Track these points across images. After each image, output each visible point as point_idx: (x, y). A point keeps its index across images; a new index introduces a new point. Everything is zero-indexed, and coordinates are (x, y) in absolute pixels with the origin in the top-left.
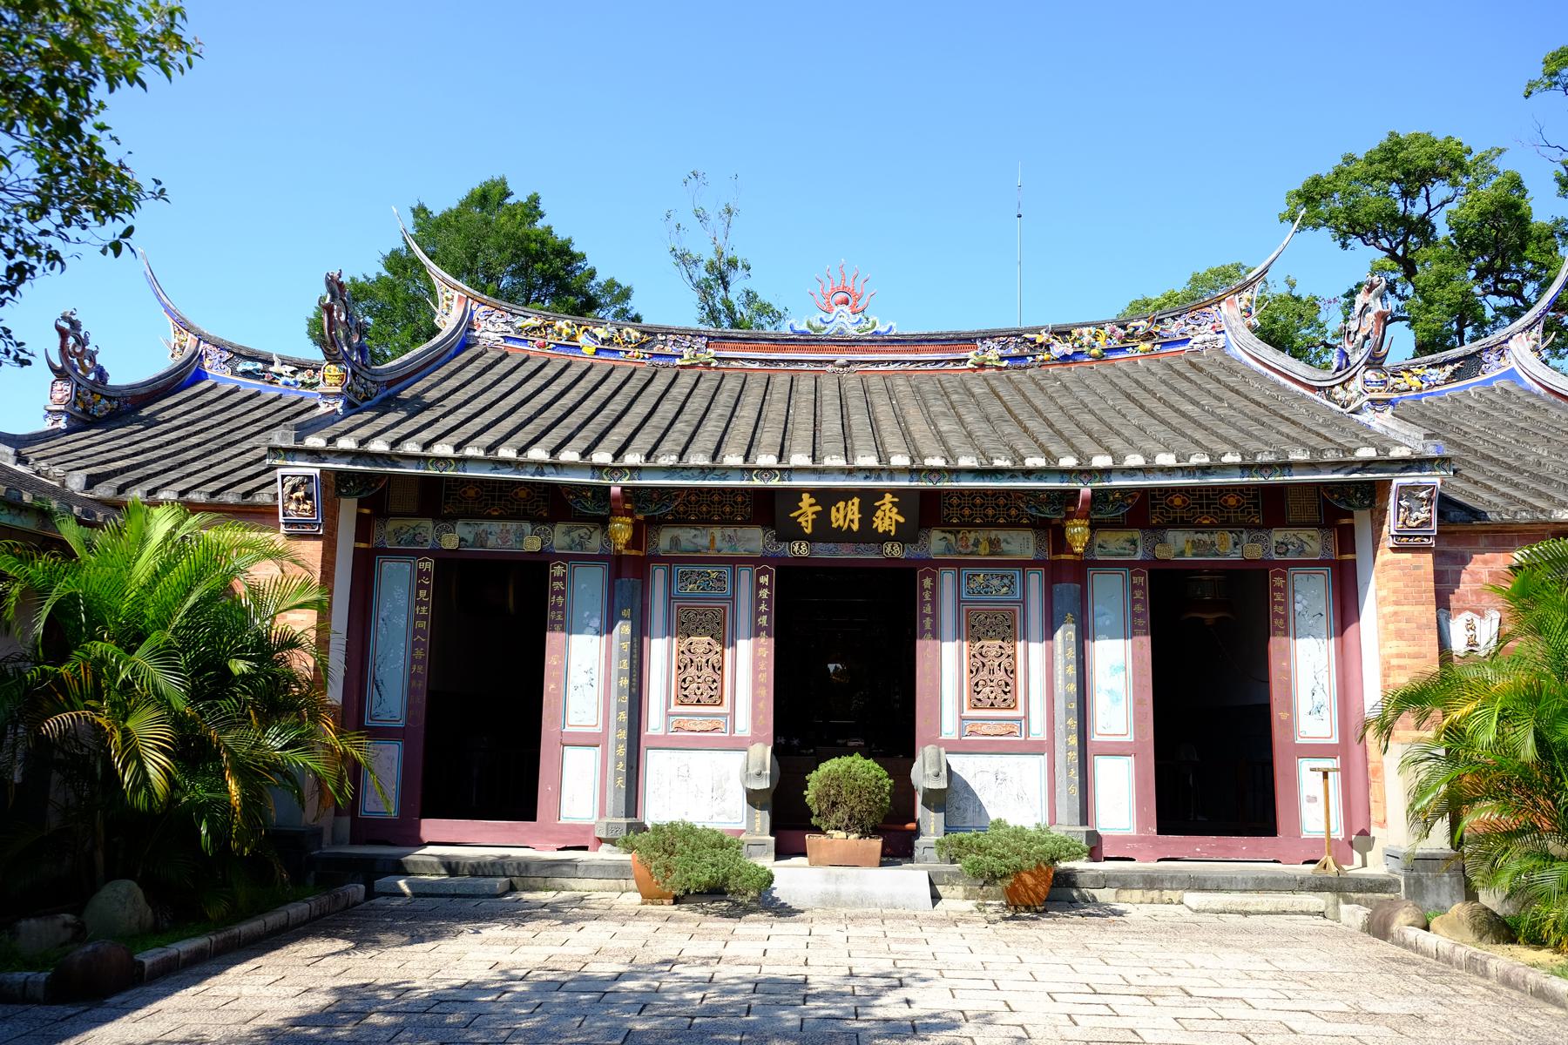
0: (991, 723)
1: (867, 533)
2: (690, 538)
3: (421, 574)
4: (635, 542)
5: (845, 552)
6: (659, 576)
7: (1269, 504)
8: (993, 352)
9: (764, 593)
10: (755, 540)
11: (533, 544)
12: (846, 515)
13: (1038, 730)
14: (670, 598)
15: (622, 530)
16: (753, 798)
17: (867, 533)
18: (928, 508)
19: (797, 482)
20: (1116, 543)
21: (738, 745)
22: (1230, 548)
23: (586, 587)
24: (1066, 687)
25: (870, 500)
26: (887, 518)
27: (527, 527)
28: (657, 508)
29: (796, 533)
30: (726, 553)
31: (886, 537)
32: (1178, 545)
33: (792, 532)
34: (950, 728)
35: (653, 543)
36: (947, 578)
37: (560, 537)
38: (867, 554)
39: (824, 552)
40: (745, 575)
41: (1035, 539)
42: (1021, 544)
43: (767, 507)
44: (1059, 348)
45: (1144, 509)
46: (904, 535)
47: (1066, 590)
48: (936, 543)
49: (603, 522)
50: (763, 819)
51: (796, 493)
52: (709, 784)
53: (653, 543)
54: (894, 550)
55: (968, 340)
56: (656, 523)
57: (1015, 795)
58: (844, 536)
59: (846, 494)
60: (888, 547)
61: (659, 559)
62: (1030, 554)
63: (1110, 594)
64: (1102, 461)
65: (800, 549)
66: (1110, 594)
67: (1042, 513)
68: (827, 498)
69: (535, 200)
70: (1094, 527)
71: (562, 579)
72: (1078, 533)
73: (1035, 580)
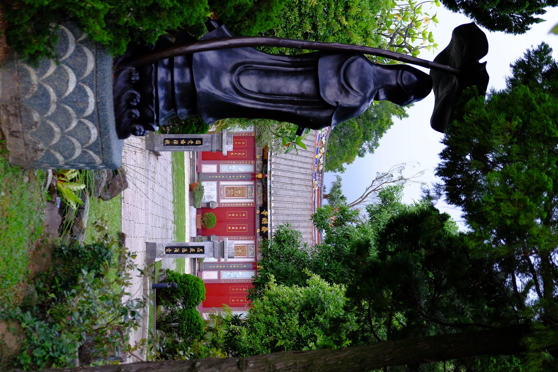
2: (260, 189)
3: (251, 133)
4: (258, 178)
6: (252, 183)
9: (249, 205)
10: (259, 203)
11: (258, 157)
12: (264, 221)
14: (247, 185)
19: (269, 211)
21: (218, 199)
25: (266, 225)
27: (261, 155)
30: (257, 197)
31: (261, 229)
36: (253, 242)
37: (259, 162)
40: (252, 201)
47: (251, 266)
49: (262, 172)
50: (204, 206)
54: (258, 231)
58: (261, 221)
60: (259, 230)
61: (255, 183)
62: (258, 259)
68: (267, 217)
69: (406, 116)
71: (251, 163)
73: (253, 260)
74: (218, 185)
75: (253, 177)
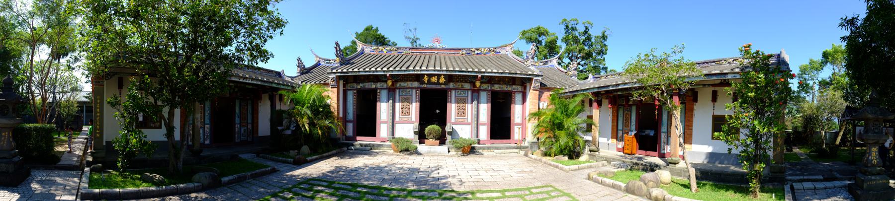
0: (461, 119)
1: (438, 83)
2: (403, 84)
4: (393, 85)
5: (434, 86)
7: (512, 81)
8: (464, 52)
10: (416, 84)
11: (374, 86)
12: (434, 79)
13: (469, 120)
15: (390, 83)
16: (415, 133)
17: (438, 83)
18: (450, 78)
20: (485, 86)
21: (412, 123)
22: (506, 88)
23: (384, 94)
24: (475, 113)
25: (439, 76)
26: (442, 80)
28: (397, 79)
29: (423, 83)
32: (496, 87)
33: (423, 83)
34: (453, 120)
35: (396, 84)
36: (453, 92)
37: (379, 85)
38: (438, 87)
39: (429, 86)
41: (470, 84)
42: (467, 86)
43: (418, 78)
44: (477, 52)
45: (490, 80)
46: (445, 83)
47: (475, 95)
48: (451, 85)
49: (386, 82)
50: (417, 137)
51: (424, 75)
52: (407, 130)
53: (396, 84)
54: (443, 86)
55: (460, 49)
56: (397, 81)
57: (465, 133)
58: (434, 83)
59: (434, 75)
63: (484, 96)
64: (483, 70)
65: (425, 86)
66: (484, 96)
67: (471, 79)
68: (430, 76)
70: (481, 83)
72: (478, 84)
73: (470, 93)
74: (399, 123)
75: (391, 92)
